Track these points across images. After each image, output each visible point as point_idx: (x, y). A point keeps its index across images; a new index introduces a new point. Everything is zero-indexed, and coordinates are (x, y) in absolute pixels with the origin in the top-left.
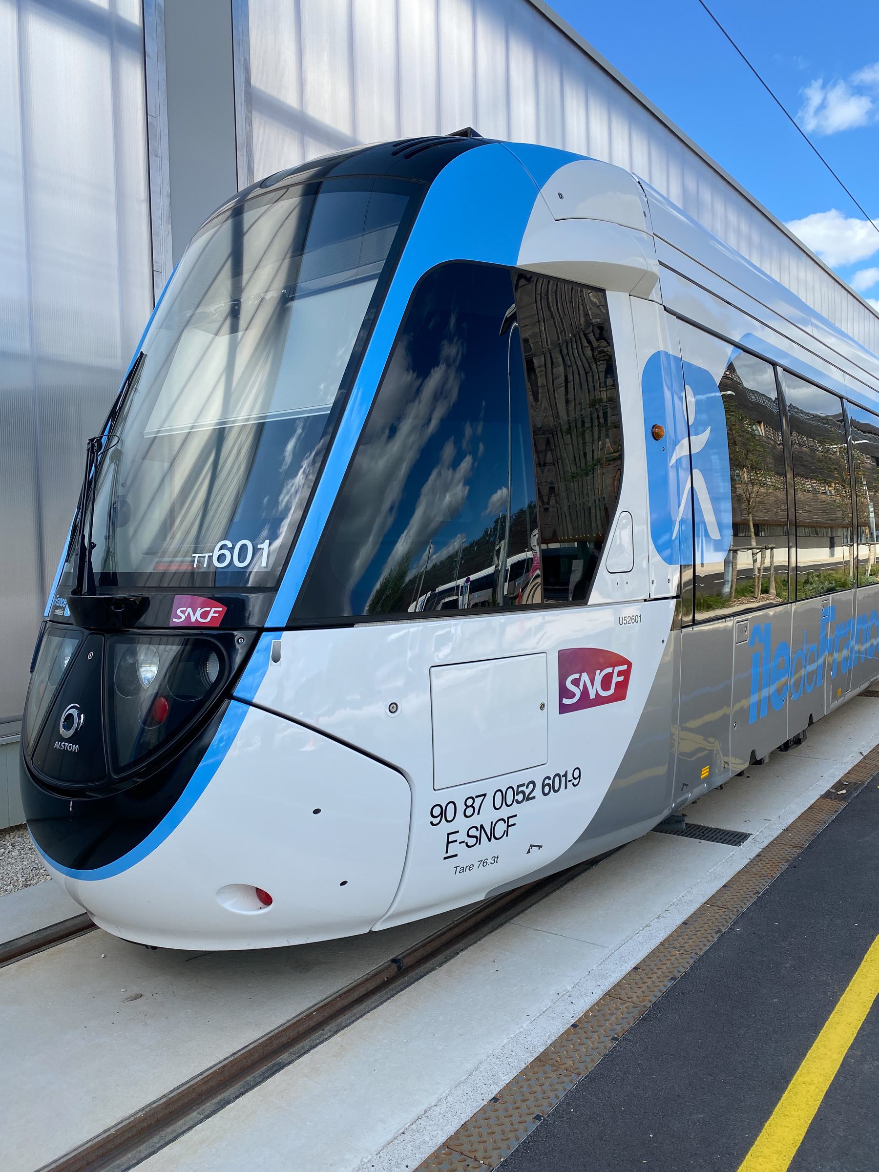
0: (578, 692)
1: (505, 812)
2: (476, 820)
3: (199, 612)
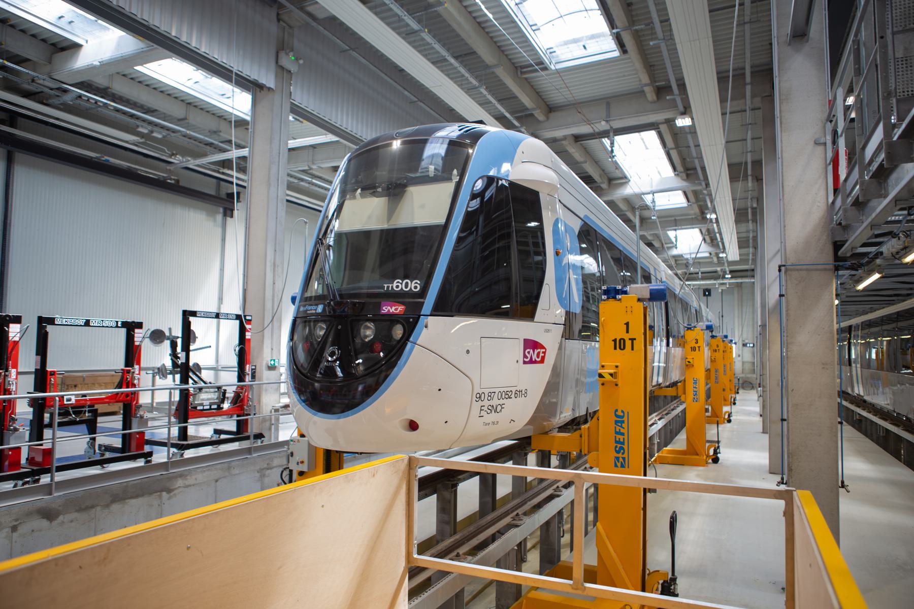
0: (529, 356)
1: (501, 402)
2: (491, 403)
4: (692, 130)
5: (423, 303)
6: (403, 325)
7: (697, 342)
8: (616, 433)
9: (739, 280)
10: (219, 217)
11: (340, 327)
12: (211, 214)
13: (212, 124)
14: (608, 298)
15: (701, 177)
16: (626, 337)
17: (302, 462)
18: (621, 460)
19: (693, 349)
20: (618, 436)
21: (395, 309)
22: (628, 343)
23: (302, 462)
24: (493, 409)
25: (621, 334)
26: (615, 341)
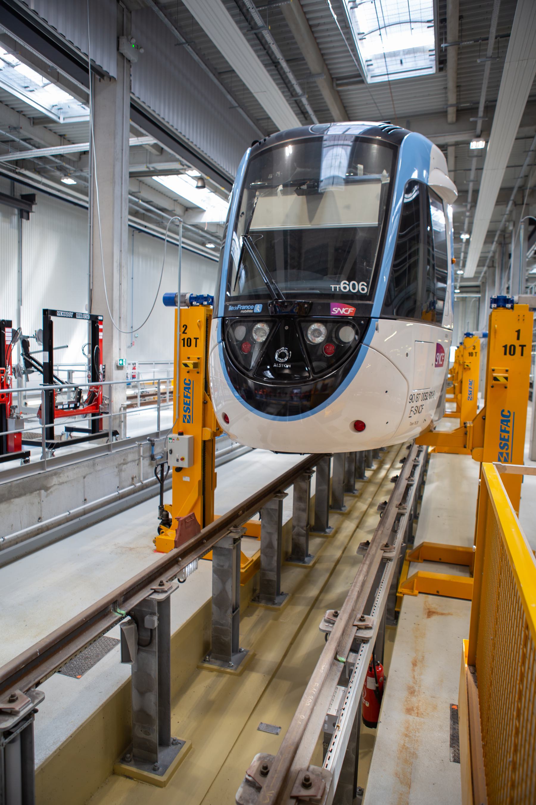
3: (344, 310)
4: (481, 154)
5: (372, 305)
6: (354, 327)
7: (474, 349)
8: (502, 431)
9: (464, 295)
10: (15, 219)
11: (287, 328)
12: (7, 215)
13: (12, 119)
14: (498, 306)
15: (470, 199)
16: (517, 343)
17: (182, 459)
18: (505, 455)
19: (471, 354)
20: (503, 434)
21: (348, 311)
22: (518, 350)
23: (182, 459)
24: (418, 410)
25: (512, 340)
26: (505, 347)
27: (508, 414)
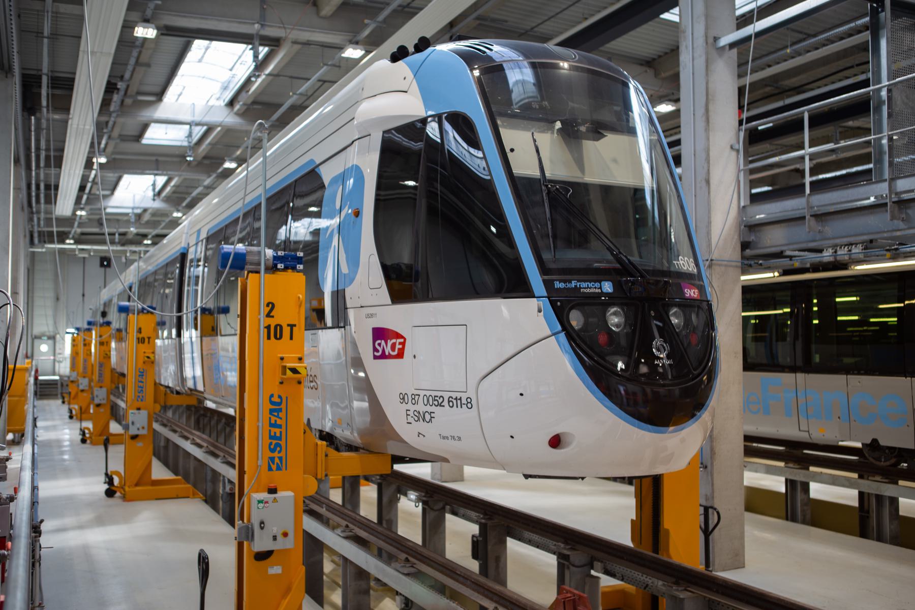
8: (271, 425)
18: (277, 460)
20: (273, 430)
22: (286, 331)
27: (279, 400)
